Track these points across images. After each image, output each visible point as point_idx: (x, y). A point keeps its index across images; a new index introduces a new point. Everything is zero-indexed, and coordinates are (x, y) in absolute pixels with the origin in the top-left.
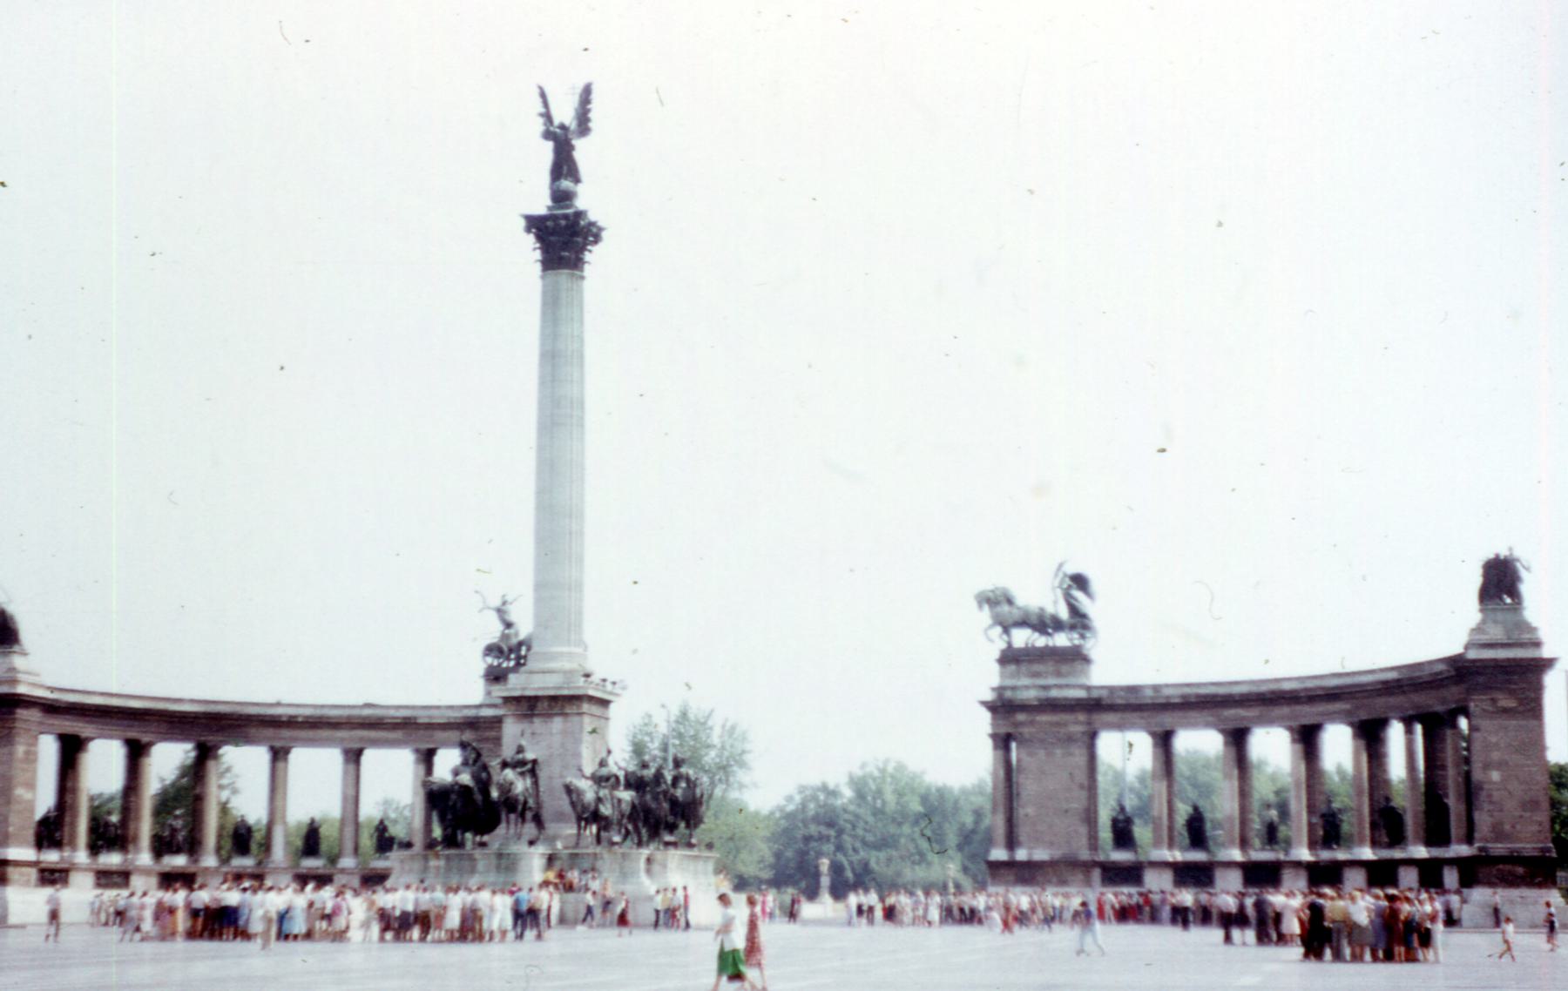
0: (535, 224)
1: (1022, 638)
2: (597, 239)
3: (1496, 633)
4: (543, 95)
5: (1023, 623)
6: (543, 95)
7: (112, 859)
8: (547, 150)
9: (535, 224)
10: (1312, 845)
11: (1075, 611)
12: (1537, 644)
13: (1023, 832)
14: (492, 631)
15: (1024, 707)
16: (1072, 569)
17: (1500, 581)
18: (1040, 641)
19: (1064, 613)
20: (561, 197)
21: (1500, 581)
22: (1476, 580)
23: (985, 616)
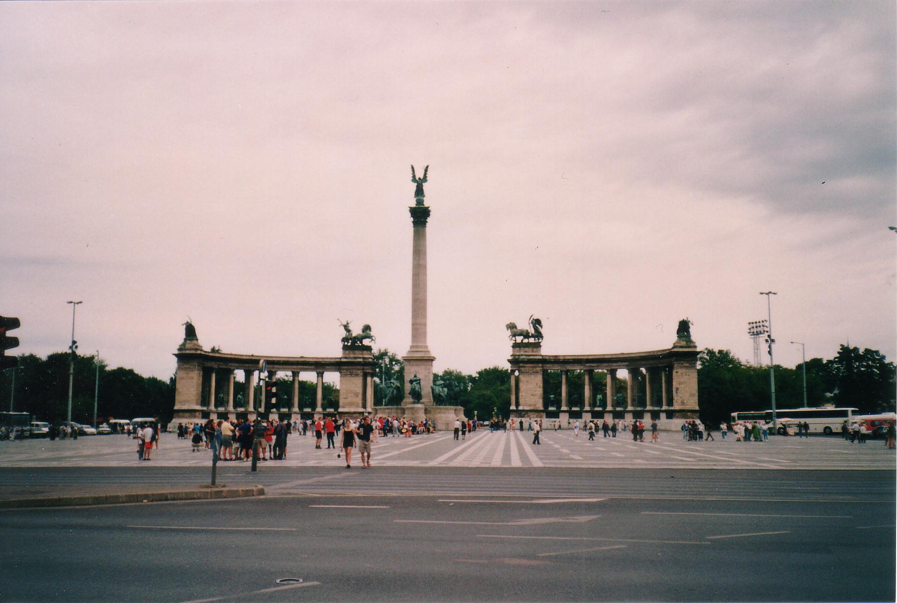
1: (519, 339)
2: (429, 215)
3: (683, 343)
4: (413, 168)
5: (520, 335)
6: (413, 168)
7: (221, 409)
10: (613, 406)
11: (536, 330)
12: (695, 347)
13: (521, 401)
14: (344, 333)
15: (523, 362)
17: (684, 328)
18: (526, 341)
20: (420, 202)
21: (684, 328)
22: (676, 327)
23: (509, 332)
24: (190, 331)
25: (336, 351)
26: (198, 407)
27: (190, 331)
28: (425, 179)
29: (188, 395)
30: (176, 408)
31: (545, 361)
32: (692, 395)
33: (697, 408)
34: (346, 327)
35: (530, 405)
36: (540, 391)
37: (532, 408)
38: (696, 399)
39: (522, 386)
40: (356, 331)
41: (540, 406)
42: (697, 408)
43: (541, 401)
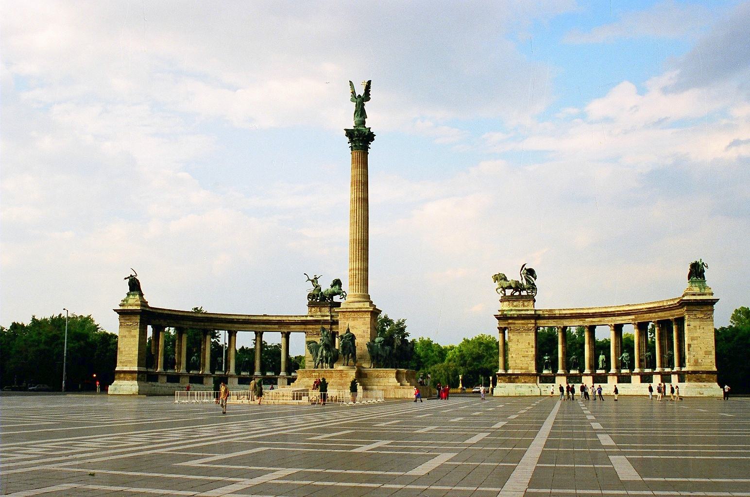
0: (349, 133)
5: (510, 287)
8: (353, 106)
9: (349, 133)
13: (511, 363)
16: (527, 267)
17: (697, 272)
21: (697, 272)
23: (497, 285)
24: (134, 285)
25: (300, 309)
26: (143, 369)
27: (134, 285)
28: (367, 96)
29: (128, 356)
30: (117, 369)
31: (537, 317)
32: (707, 353)
33: (715, 369)
34: (314, 281)
35: (522, 369)
36: (532, 352)
37: (523, 371)
38: (712, 357)
39: (512, 346)
41: (533, 370)
42: (715, 369)
43: (533, 363)
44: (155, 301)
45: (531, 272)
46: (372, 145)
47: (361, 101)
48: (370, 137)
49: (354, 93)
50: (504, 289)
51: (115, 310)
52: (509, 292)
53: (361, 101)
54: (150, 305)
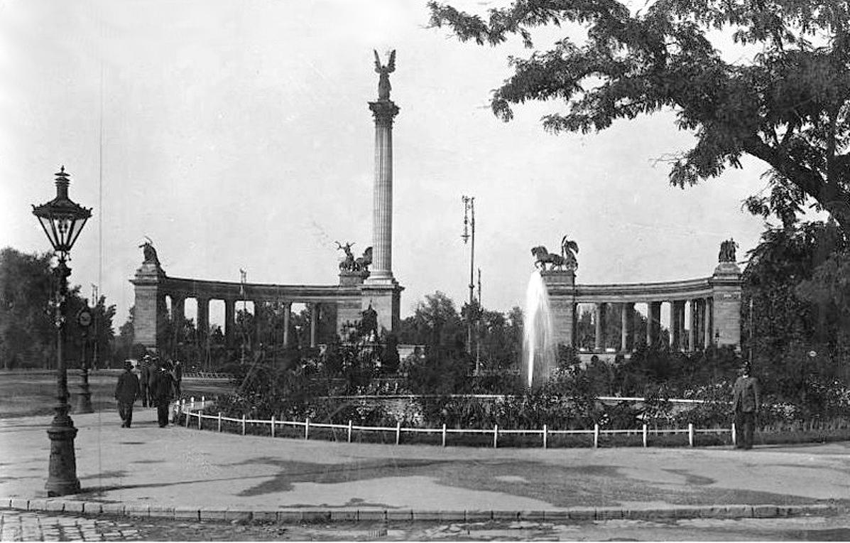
0: (372, 106)
4: (375, 52)
8: (377, 77)
9: (372, 106)
16: (569, 239)
19: (565, 256)
23: (535, 258)
24: (150, 253)
27: (150, 253)
28: (392, 66)
40: (358, 253)
44: (173, 270)
45: (572, 245)
46: (396, 119)
47: (385, 72)
48: (395, 110)
49: (377, 63)
50: (543, 263)
51: (130, 281)
52: (548, 266)
53: (385, 72)
54: (168, 275)
